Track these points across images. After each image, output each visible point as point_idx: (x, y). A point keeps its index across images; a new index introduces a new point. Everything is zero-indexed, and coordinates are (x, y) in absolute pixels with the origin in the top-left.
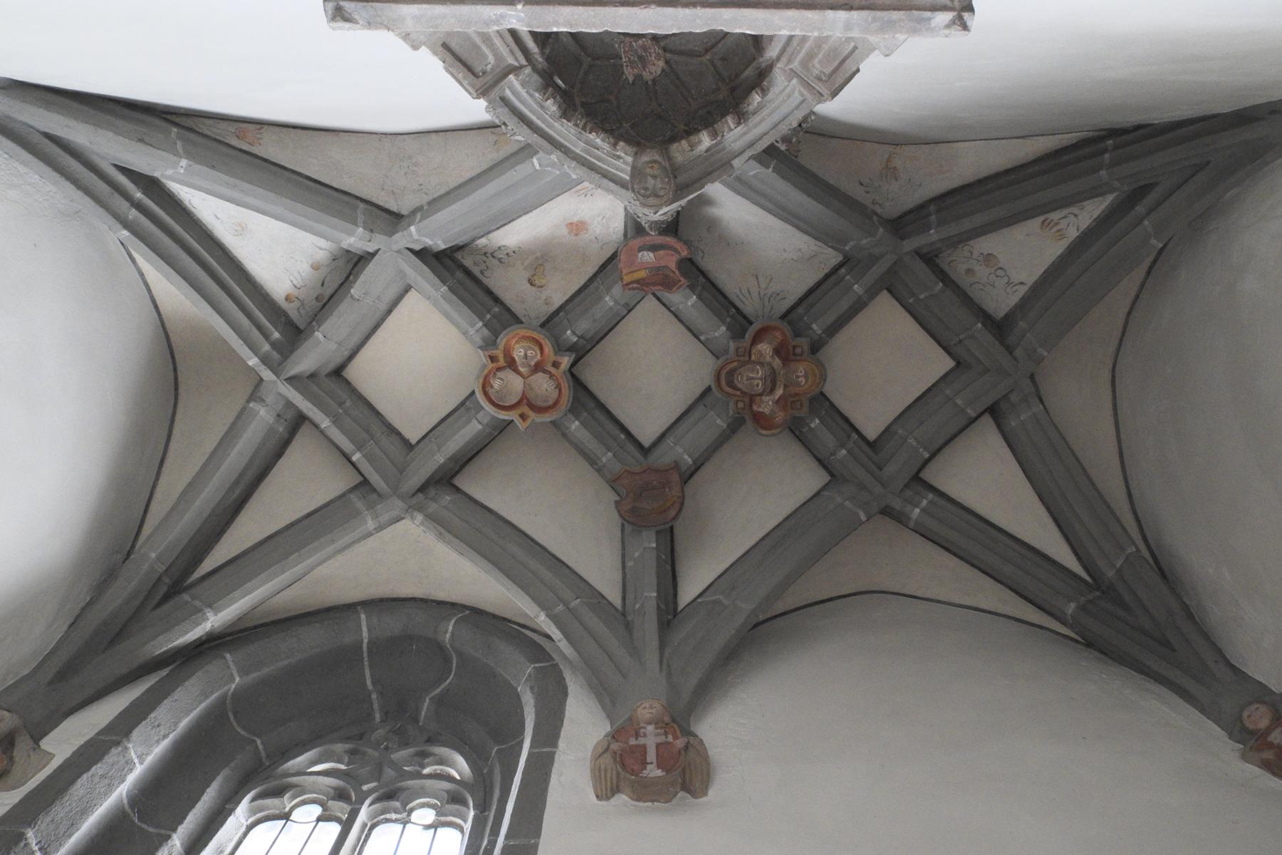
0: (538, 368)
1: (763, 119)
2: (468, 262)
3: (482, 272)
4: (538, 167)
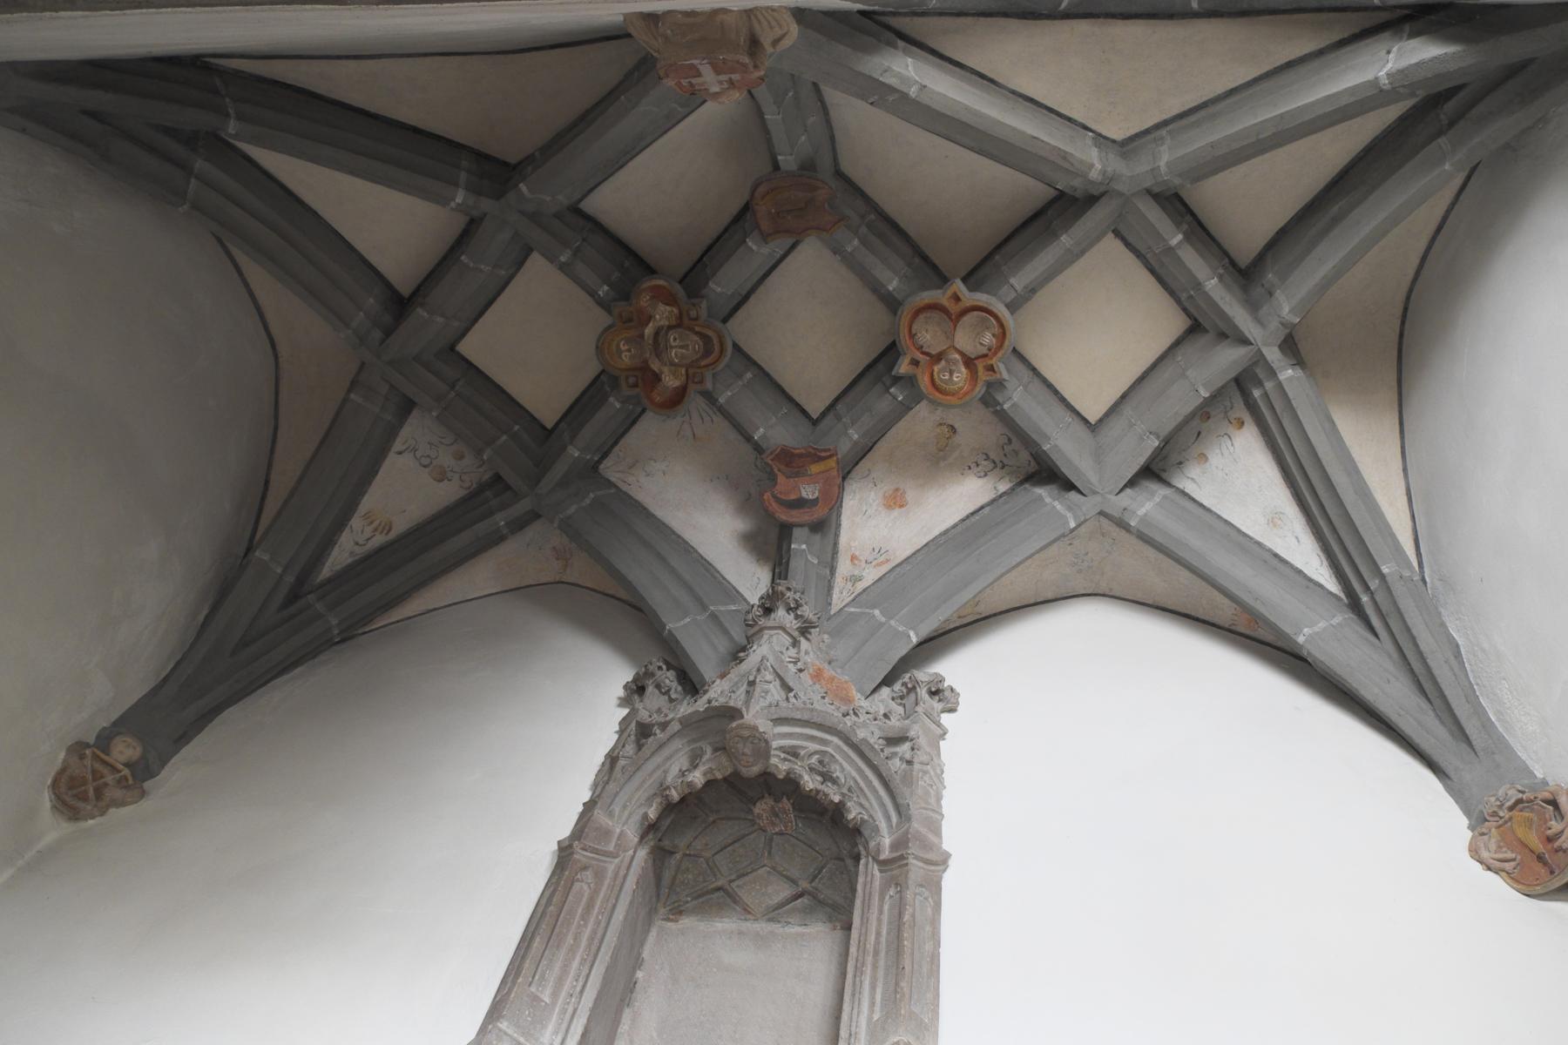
0: (938, 358)
1: (650, 775)
3: (1010, 440)
4: (912, 634)
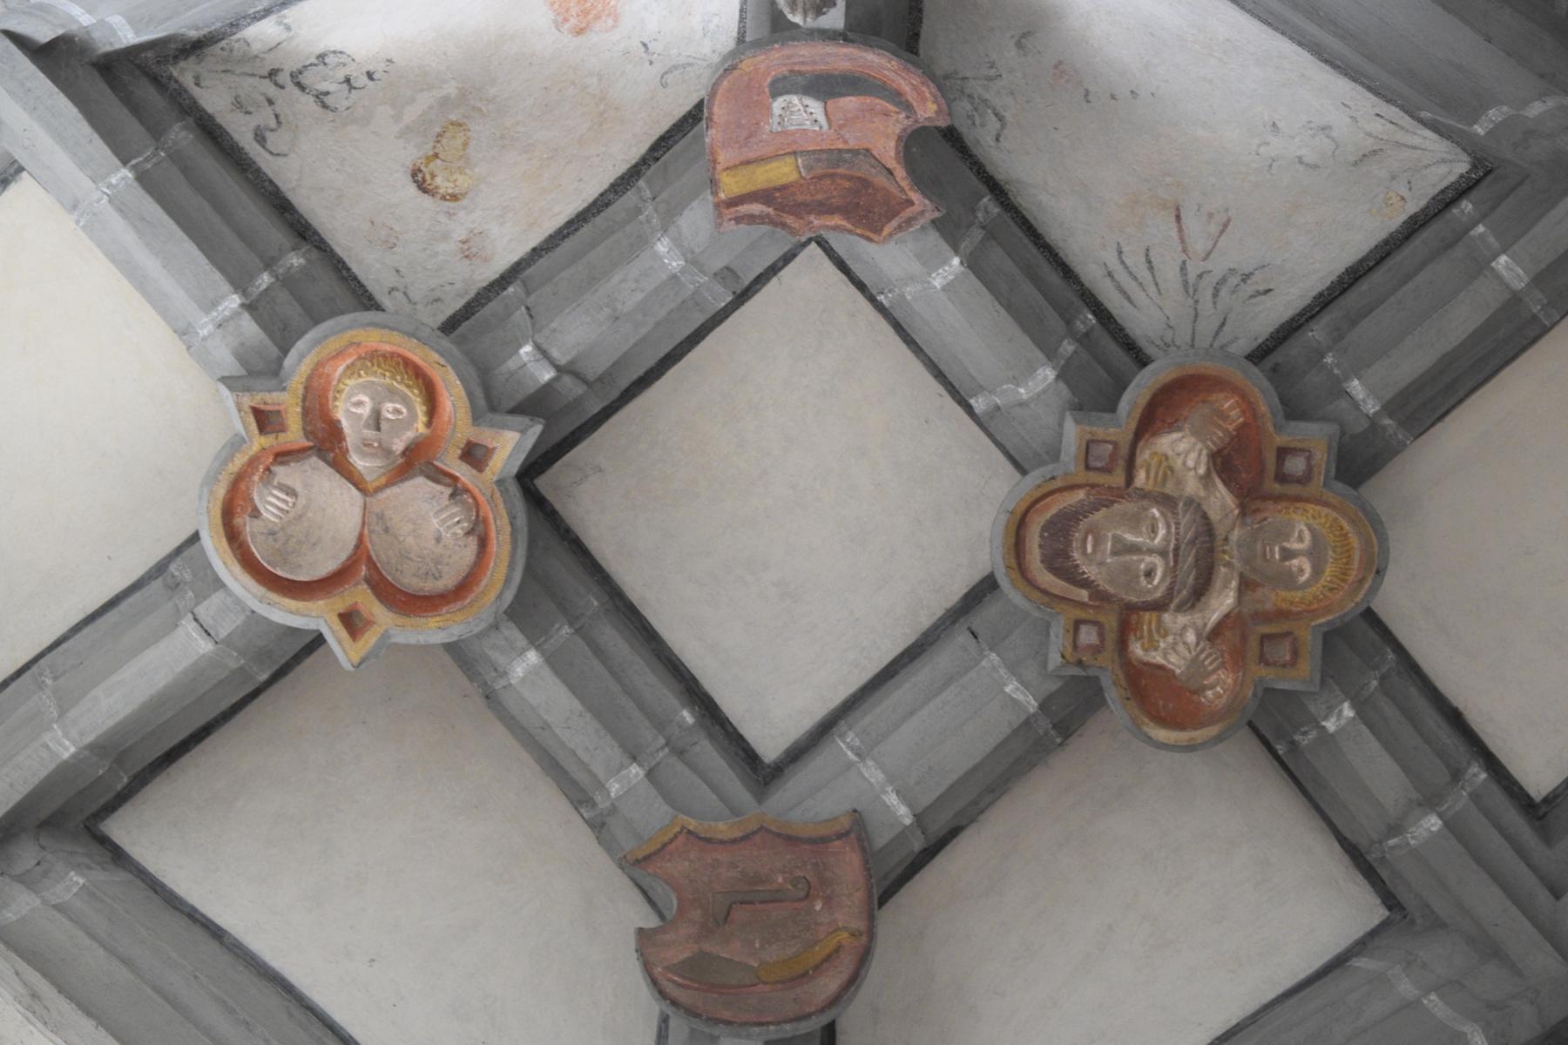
0: (415, 460)
2: (214, 99)
3: (260, 137)
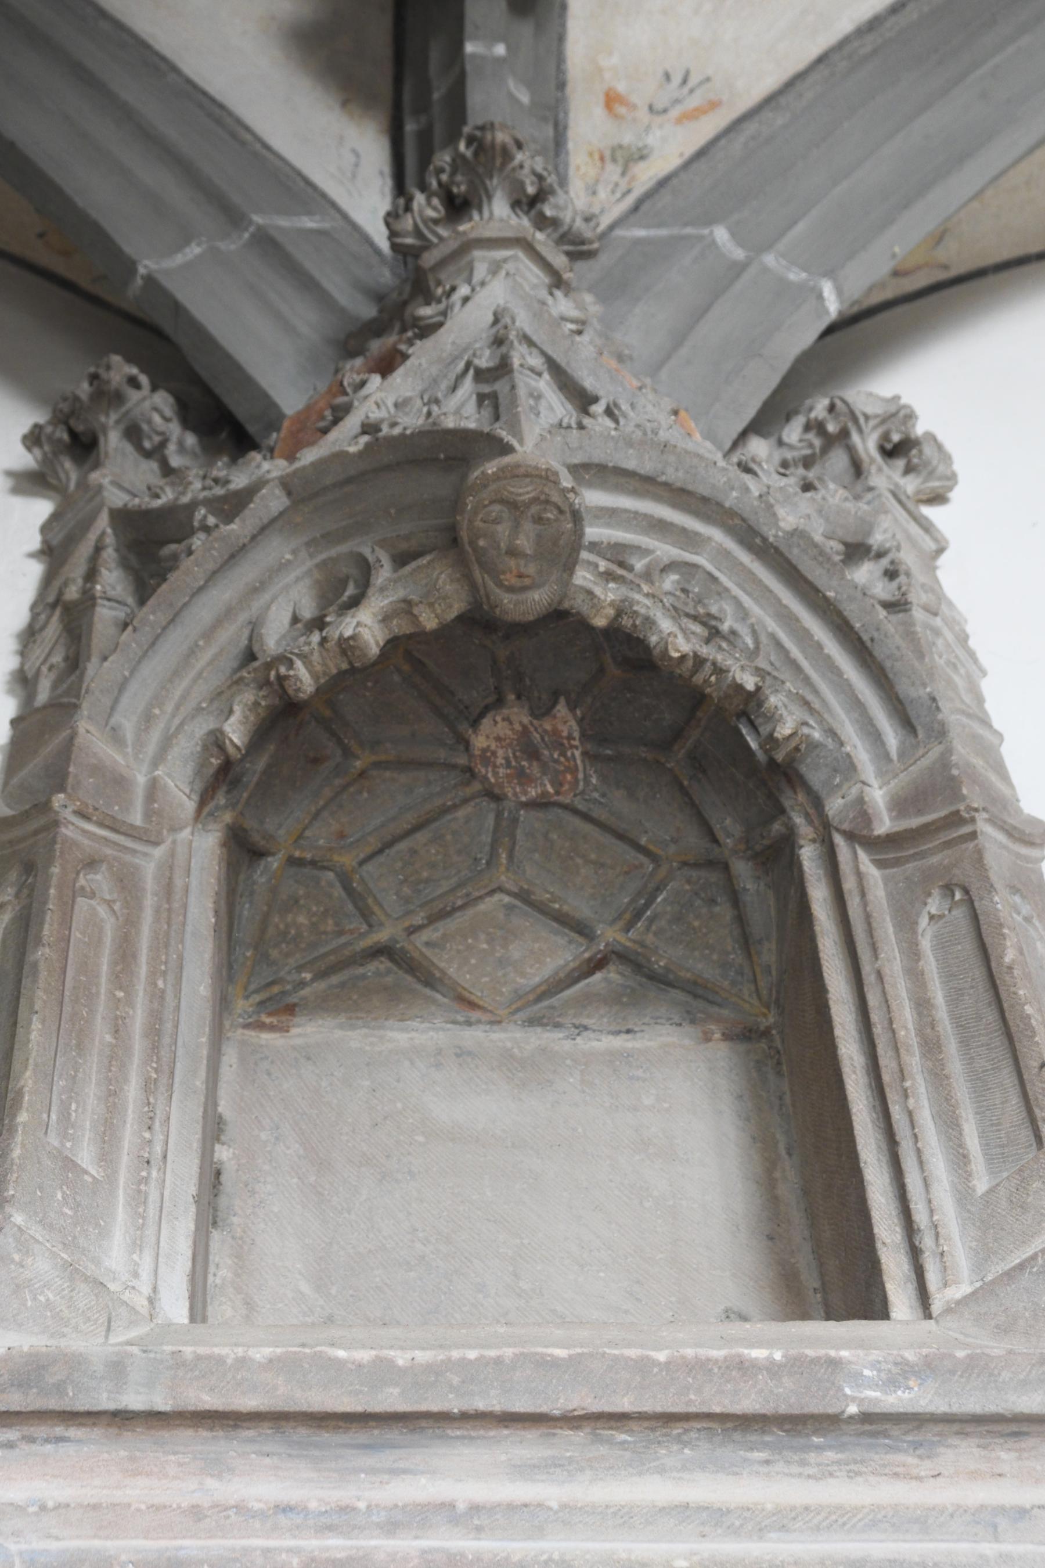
1: (208, 634)
